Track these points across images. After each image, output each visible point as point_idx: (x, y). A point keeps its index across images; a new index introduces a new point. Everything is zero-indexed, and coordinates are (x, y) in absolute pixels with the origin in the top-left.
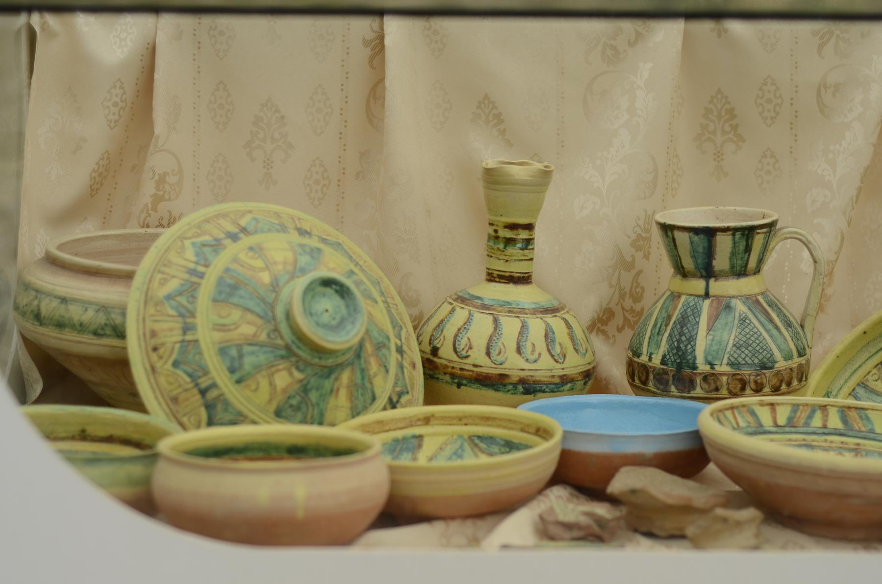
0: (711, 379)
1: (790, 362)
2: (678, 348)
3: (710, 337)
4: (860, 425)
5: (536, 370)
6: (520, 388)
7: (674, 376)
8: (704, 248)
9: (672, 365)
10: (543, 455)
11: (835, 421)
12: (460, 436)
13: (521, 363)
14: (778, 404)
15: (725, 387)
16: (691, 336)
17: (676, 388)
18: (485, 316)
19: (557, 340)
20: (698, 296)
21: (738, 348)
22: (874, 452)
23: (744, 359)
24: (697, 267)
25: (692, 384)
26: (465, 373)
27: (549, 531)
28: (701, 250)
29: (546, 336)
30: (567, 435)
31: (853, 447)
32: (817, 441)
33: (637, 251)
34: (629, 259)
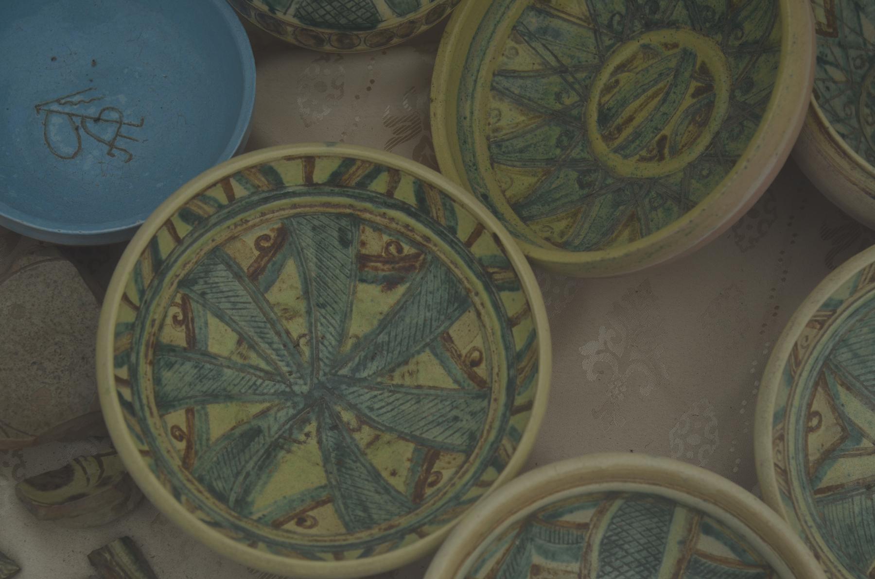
4: (441, 214)
22: (444, 264)
23: (323, 16)
31: (419, 238)
32: (371, 213)
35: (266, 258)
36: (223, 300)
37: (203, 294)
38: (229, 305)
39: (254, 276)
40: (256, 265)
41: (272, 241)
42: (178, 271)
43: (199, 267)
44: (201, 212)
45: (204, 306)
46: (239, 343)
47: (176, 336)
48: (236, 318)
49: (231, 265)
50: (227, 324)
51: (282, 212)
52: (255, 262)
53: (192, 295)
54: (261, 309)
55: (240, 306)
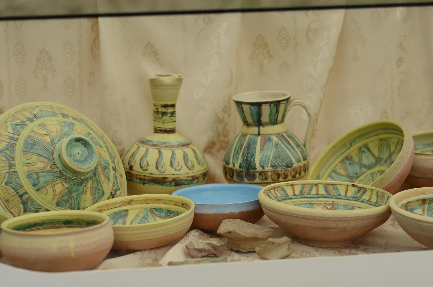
0: (263, 174)
1: (300, 163)
2: (247, 160)
3: (262, 154)
4: (334, 192)
6: (173, 184)
7: (246, 173)
8: (257, 112)
9: (245, 168)
10: (186, 217)
11: (322, 191)
12: (146, 209)
13: (172, 171)
14: (295, 185)
15: (270, 177)
16: (253, 154)
17: (247, 179)
18: (154, 149)
19: (190, 159)
20: (255, 135)
21: (275, 159)
22: (341, 205)
23: (278, 164)
24: (254, 121)
25: (254, 177)
26: (146, 178)
27: (191, 254)
28: (255, 113)
29: (184, 157)
30: (197, 206)
31: (331, 203)
34: (221, 118)
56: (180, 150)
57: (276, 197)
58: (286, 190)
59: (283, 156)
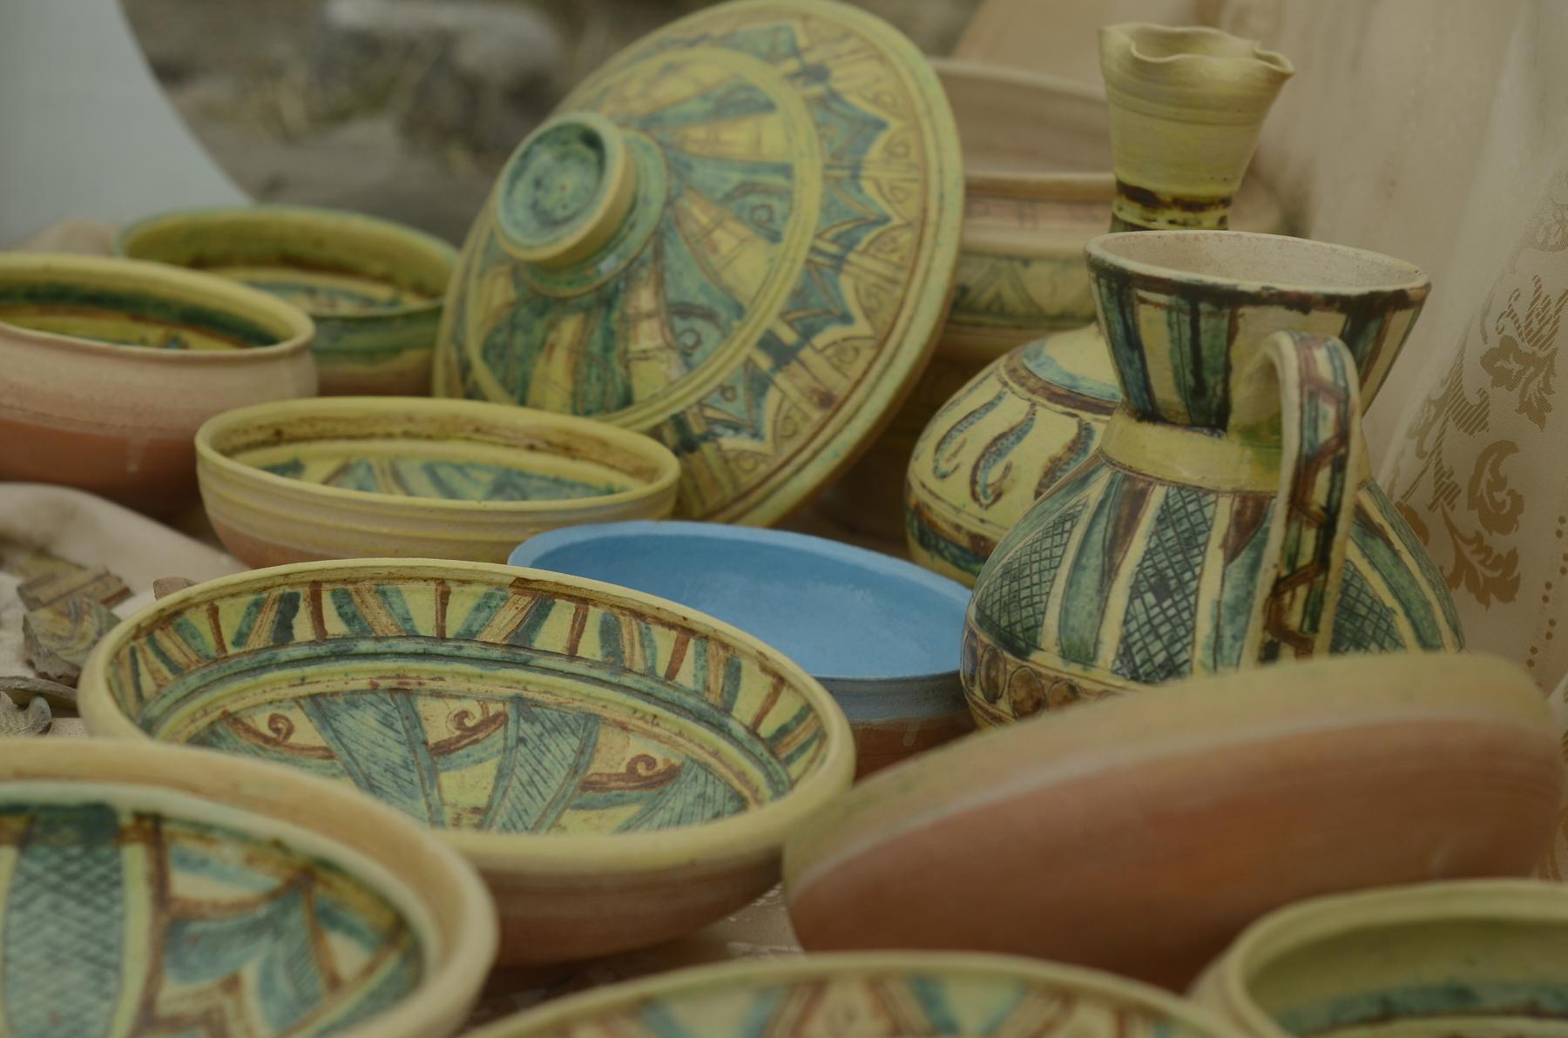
1: (1076, 669)
5: (938, 498)
14: (791, 686)
19: (1011, 457)
33: (1495, 383)
34: (1474, 400)
35: (622, 784)
36: (529, 768)
37: (521, 741)
38: (525, 778)
39: (587, 786)
40: (605, 779)
41: (650, 773)
42: (534, 683)
43: (556, 714)
44: (627, 650)
45: (505, 749)
46: (476, 810)
47: (438, 722)
48: (511, 793)
49: (587, 749)
50: (495, 788)
51: (699, 751)
52: (609, 775)
53: (511, 725)
54: (544, 815)
55: (533, 792)
56: (1025, 406)
57: (661, 671)
58: (745, 682)
59: (1027, 582)
